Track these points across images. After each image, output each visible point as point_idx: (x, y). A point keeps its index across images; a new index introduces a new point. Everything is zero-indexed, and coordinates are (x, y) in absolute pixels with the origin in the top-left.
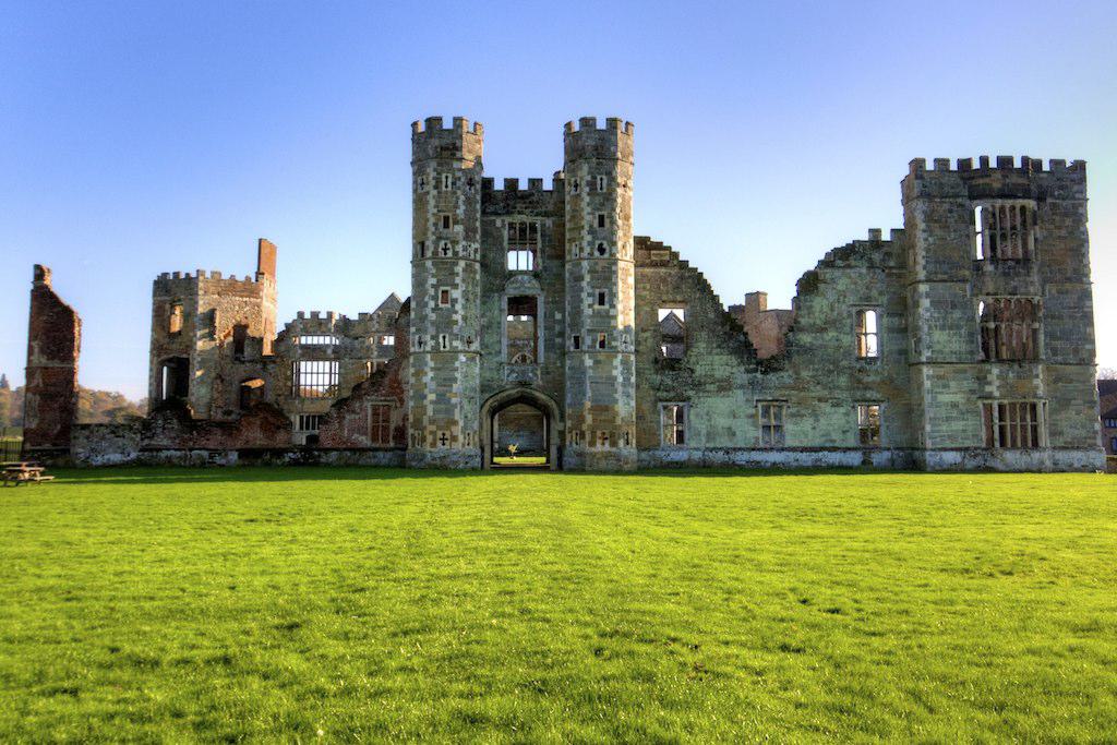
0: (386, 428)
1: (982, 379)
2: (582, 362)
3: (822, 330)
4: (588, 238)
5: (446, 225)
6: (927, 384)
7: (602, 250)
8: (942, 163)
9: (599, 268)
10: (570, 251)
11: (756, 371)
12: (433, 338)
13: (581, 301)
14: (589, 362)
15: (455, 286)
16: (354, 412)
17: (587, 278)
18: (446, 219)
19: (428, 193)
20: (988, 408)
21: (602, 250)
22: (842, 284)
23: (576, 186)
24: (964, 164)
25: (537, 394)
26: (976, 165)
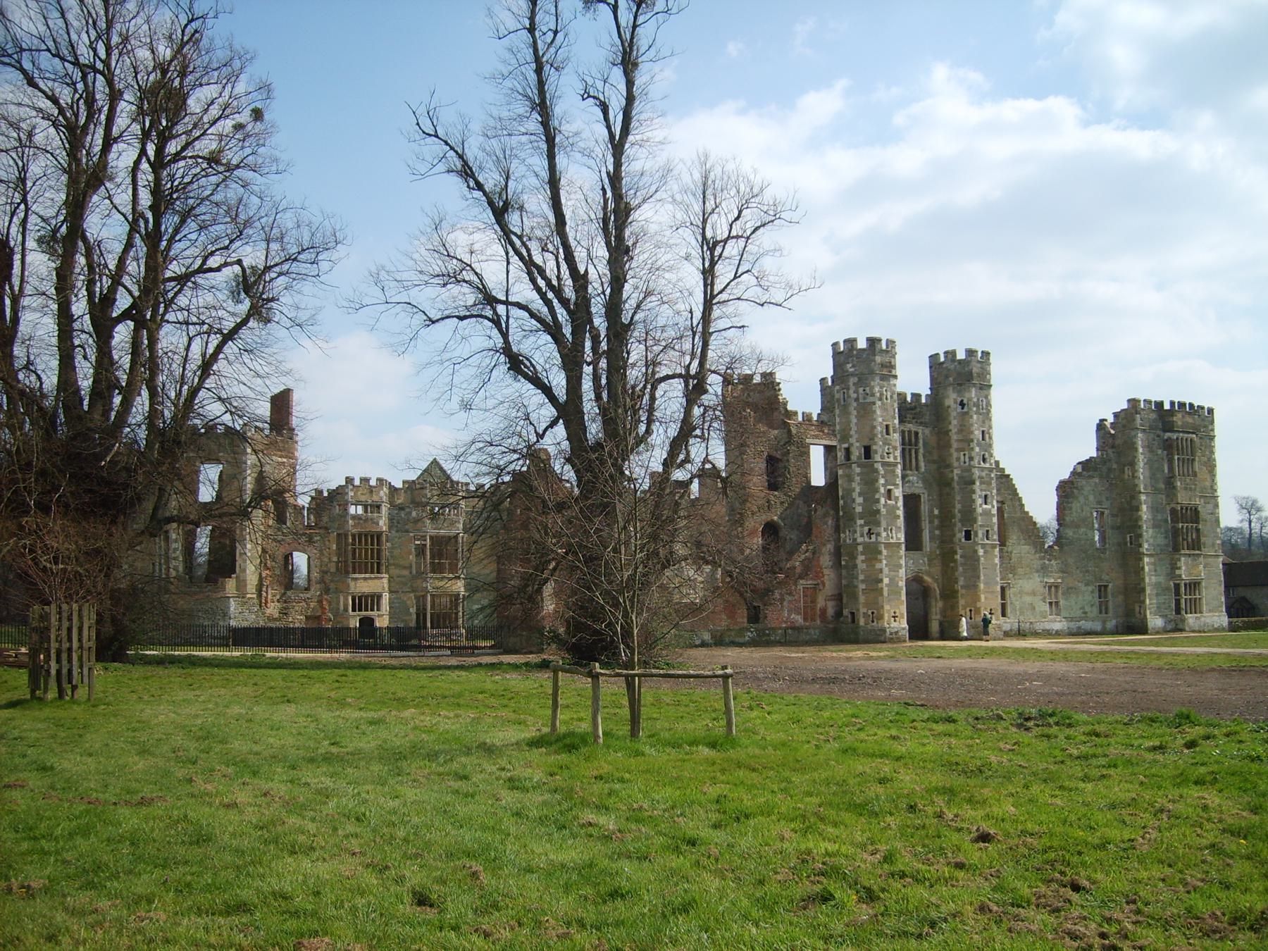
0: (813, 609)
1: (1174, 567)
2: (976, 552)
3: (1078, 527)
4: (977, 449)
5: (888, 433)
6: (1147, 568)
7: (984, 460)
8: (1150, 402)
9: (984, 474)
10: (958, 459)
11: (1043, 558)
12: (885, 530)
13: (974, 501)
14: (981, 552)
15: (896, 485)
16: (790, 594)
17: (978, 483)
18: (887, 426)
19: (874, 403)
20: (1177, 587)
21: (984, 460)
22: (1087, 488)
23: (962, 404)
24: (1160, 405)
25: (926, 578)
26: (1167, 406)
